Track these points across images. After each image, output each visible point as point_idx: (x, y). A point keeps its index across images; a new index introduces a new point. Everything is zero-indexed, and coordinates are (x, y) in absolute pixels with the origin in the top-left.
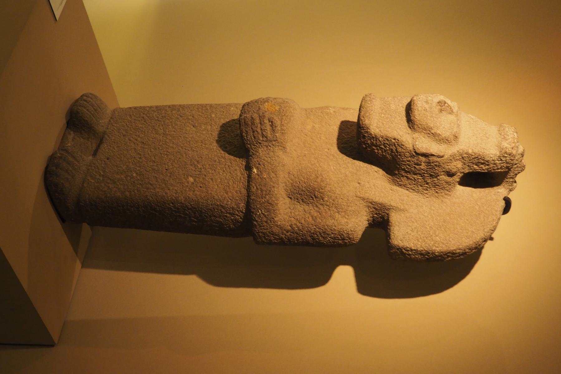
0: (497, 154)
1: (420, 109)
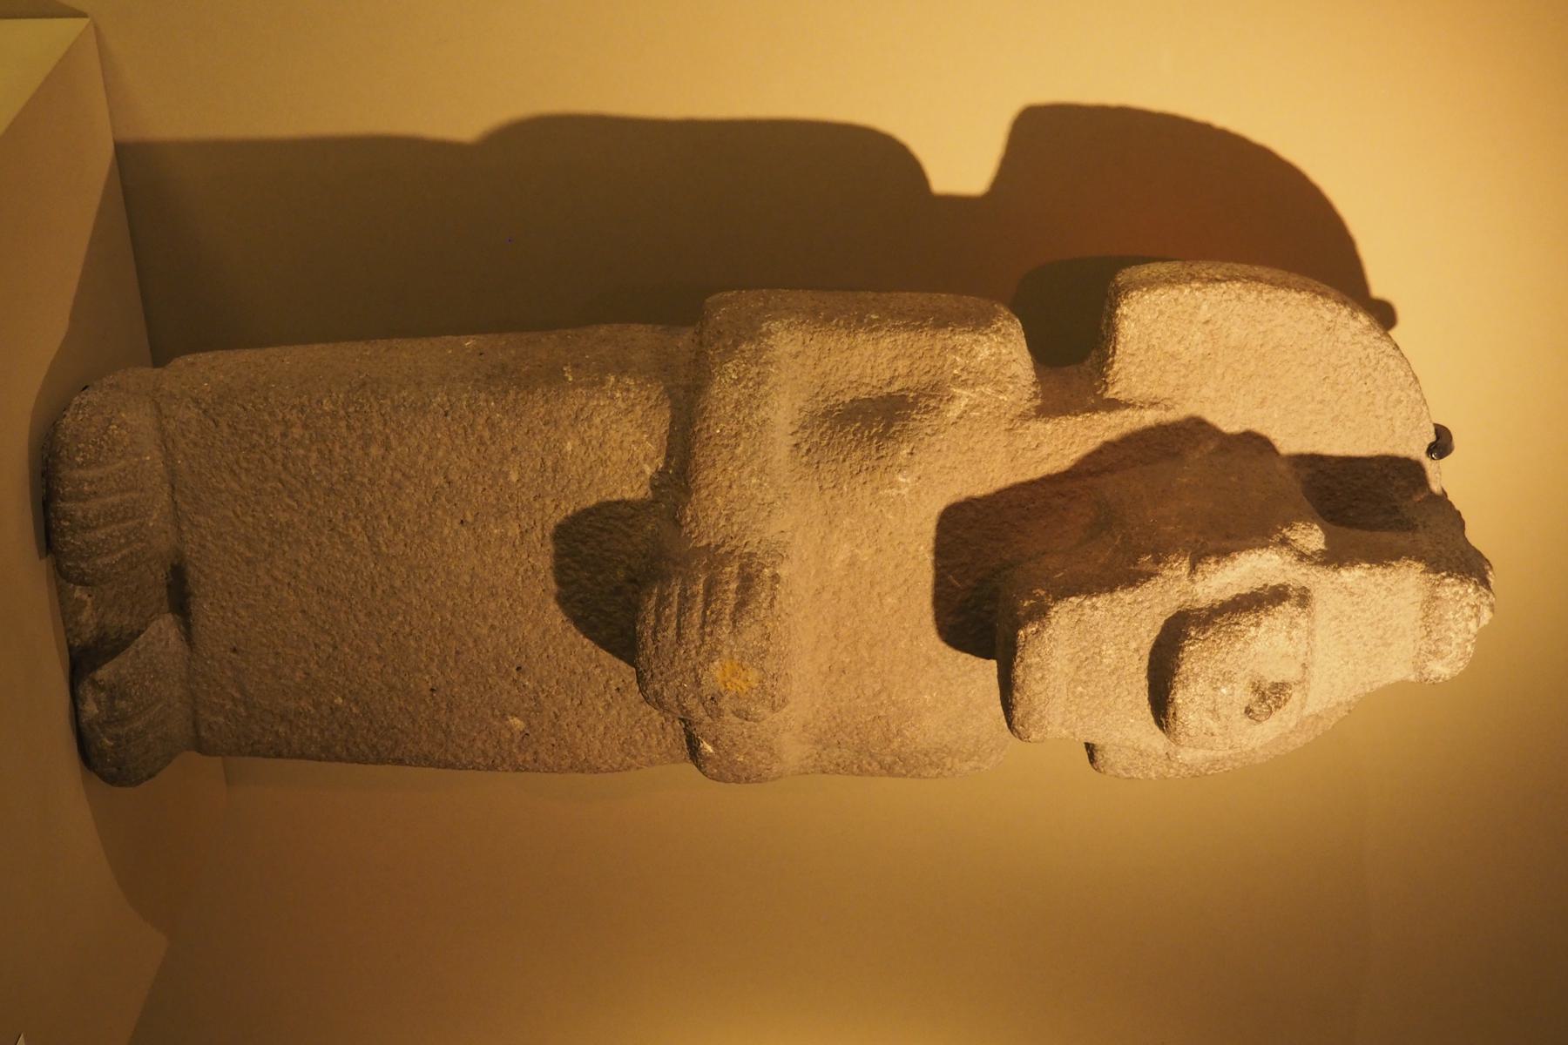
1: (1192, 733)
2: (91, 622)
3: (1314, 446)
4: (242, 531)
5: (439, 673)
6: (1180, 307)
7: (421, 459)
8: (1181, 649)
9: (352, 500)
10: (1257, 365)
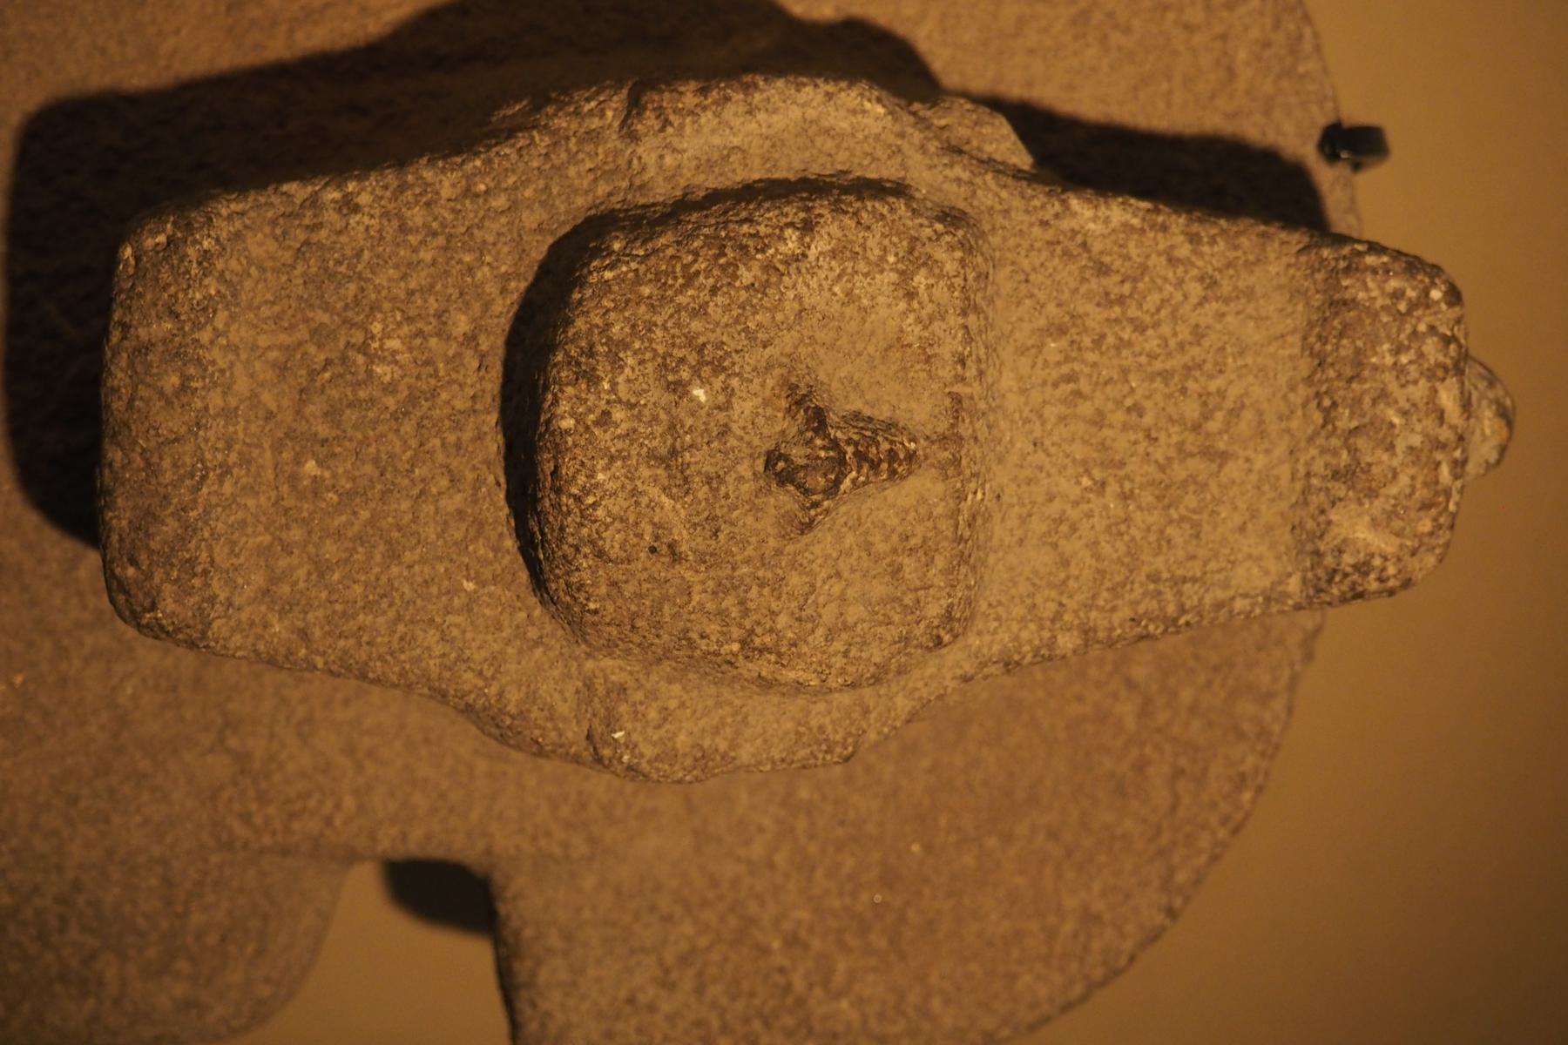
0: (1287, 595)
1: (612, 541)
3: (1029, 84)
8: (581, 283)
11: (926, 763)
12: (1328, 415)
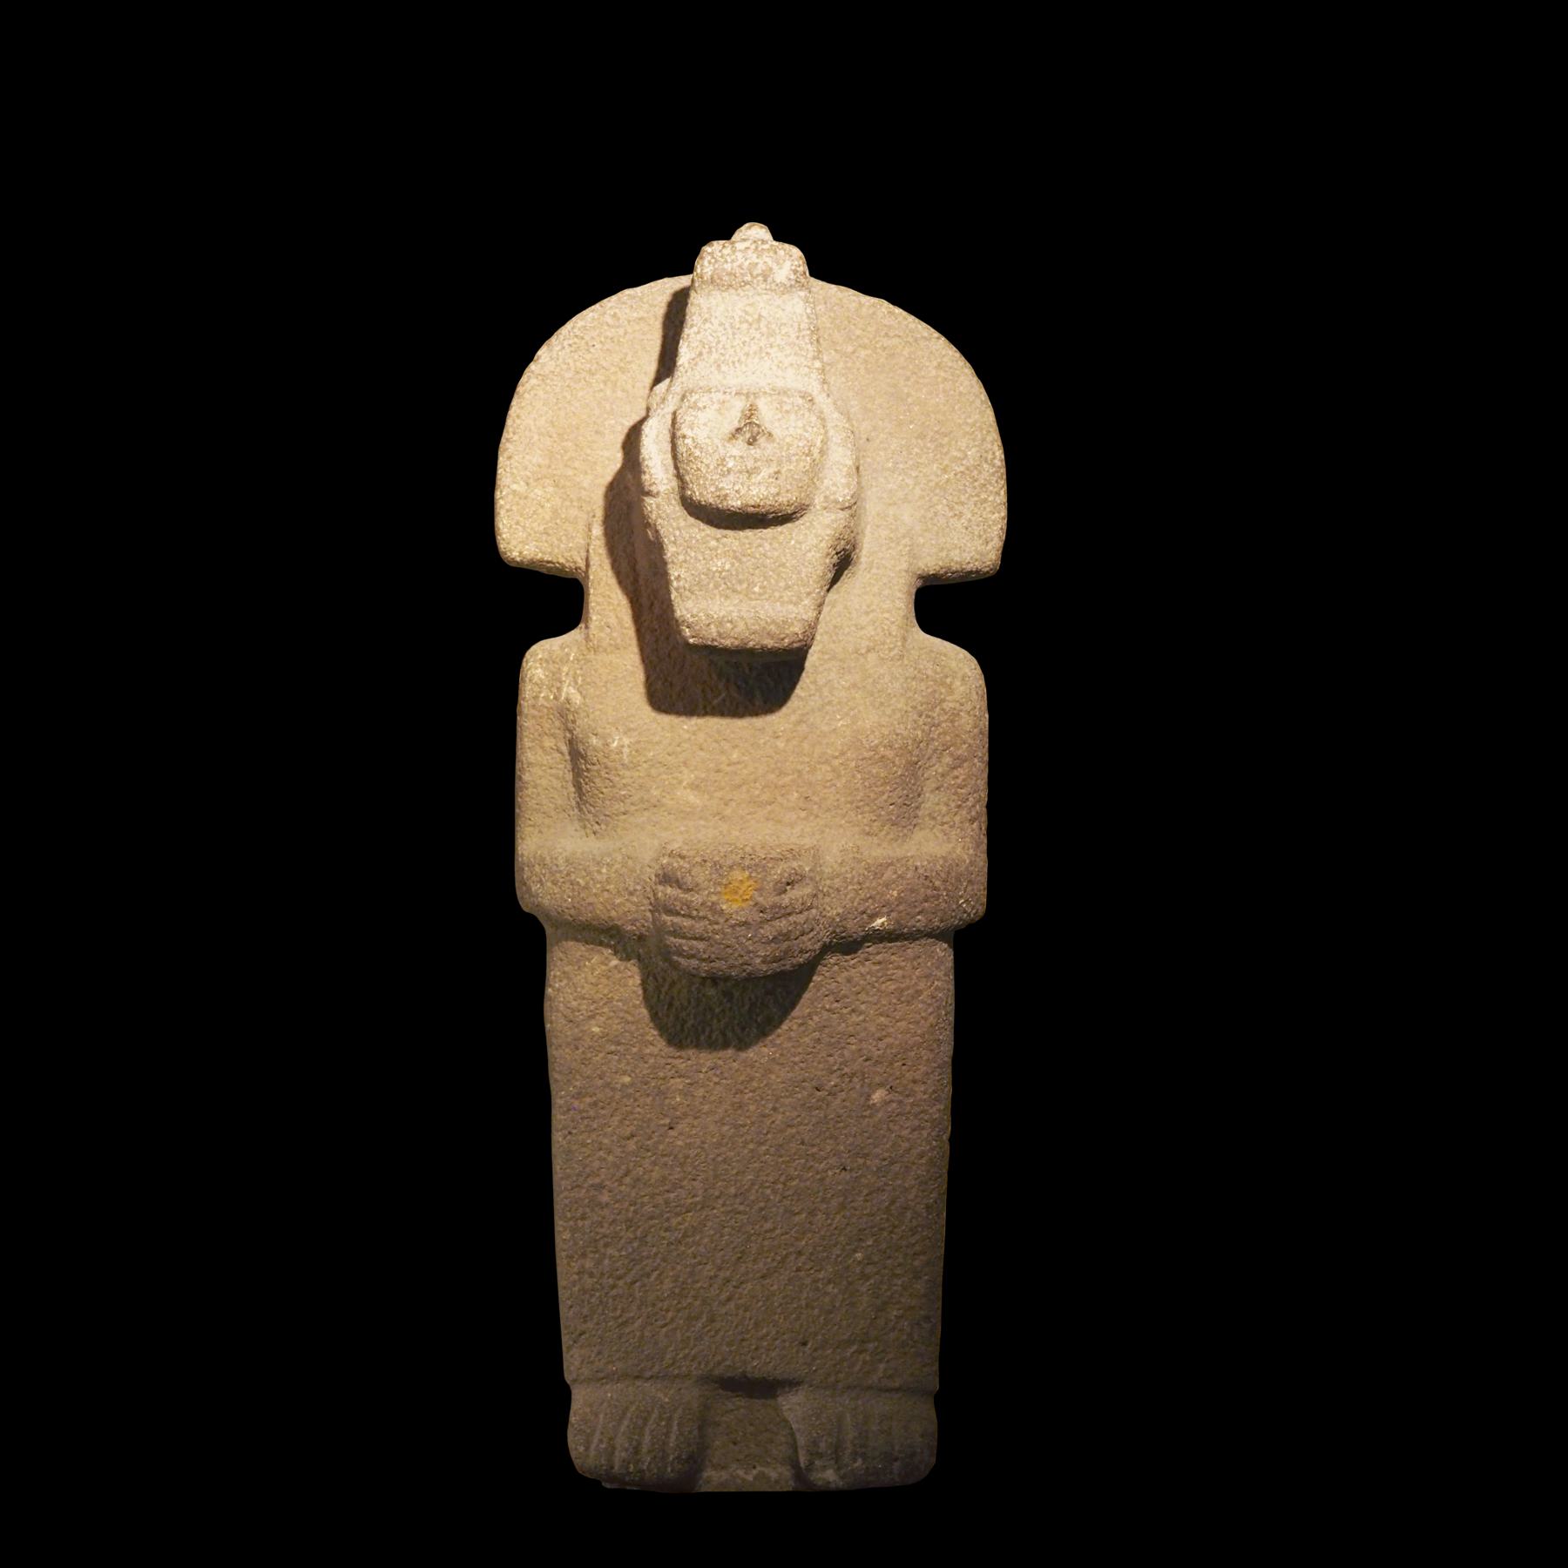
0: (806, 296)
1: (773, 490)
2: (780, 1470)
4: (681, 1322)
5: (826, 1162)
6: (514, 508)
7: (611, 1158)
8: (700, 502)
9: (651, 1222)
10: (566, 441)
11: (880, 422)
12: (747, 283)
